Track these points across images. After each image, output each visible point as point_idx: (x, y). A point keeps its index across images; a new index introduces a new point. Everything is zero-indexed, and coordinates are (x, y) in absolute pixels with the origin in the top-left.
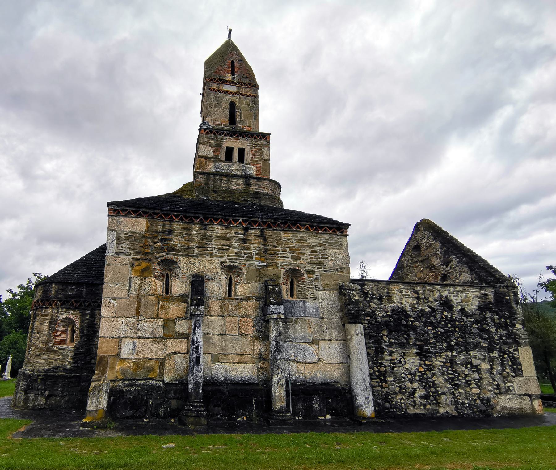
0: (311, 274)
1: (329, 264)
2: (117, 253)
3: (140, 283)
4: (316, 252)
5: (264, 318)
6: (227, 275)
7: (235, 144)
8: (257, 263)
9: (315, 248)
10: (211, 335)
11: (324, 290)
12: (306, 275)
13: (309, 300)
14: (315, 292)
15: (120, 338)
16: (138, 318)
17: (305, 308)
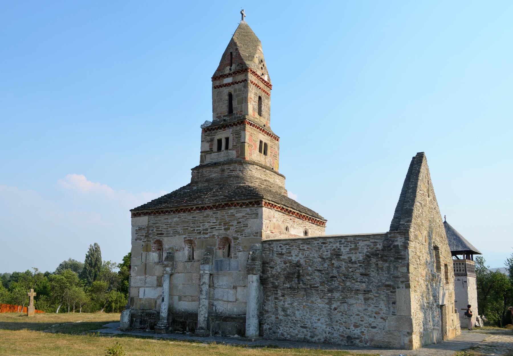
1: (247, 231)
4: (240, 223)
6: (191, 246)
7: (222, 135)
9: (240, 220)
12: (233, 241)
14: (238, 253)
15: (139, 287)
17: (229, 264)
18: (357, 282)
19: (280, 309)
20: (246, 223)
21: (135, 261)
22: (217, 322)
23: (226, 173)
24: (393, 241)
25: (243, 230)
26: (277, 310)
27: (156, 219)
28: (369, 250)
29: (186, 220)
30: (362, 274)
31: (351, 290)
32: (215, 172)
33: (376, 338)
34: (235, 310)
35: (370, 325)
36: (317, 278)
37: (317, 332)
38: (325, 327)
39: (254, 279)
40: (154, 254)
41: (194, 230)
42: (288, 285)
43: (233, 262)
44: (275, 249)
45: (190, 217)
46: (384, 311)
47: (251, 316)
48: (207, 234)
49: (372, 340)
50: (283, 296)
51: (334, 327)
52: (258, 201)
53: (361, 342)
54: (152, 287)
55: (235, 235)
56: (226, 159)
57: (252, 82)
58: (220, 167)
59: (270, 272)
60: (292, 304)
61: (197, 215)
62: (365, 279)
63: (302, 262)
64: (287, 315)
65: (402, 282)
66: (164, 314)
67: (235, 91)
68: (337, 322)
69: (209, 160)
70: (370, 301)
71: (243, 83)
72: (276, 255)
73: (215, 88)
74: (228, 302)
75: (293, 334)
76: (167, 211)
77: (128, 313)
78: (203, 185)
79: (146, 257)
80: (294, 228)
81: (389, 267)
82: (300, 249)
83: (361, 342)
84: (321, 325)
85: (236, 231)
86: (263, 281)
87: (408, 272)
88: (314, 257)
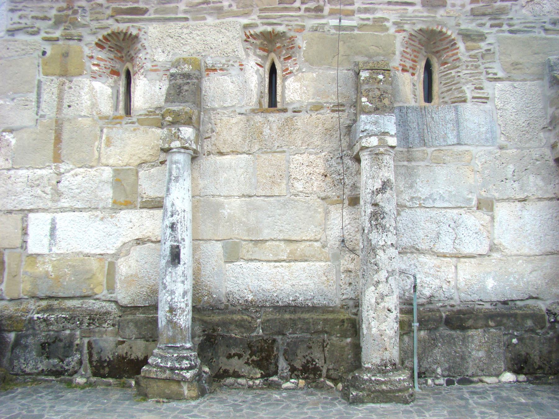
0: (473, 40)
2: (12, 32)
5: (350, 152)
6: (264, 58)
8: (334, 22)
10: (222, 199)
11: (509, 79)
12: (461, 45)
13: (468, 105)
14: (487, 85)
15: (25, 213)
16: (57, 167)
17: (457, 123)
25: (502, 11)
34: (490, 284)
40: (97, 85)
43: (473, 115)
54: (90, 209)
74: (459, 256)
79: (60, 98)
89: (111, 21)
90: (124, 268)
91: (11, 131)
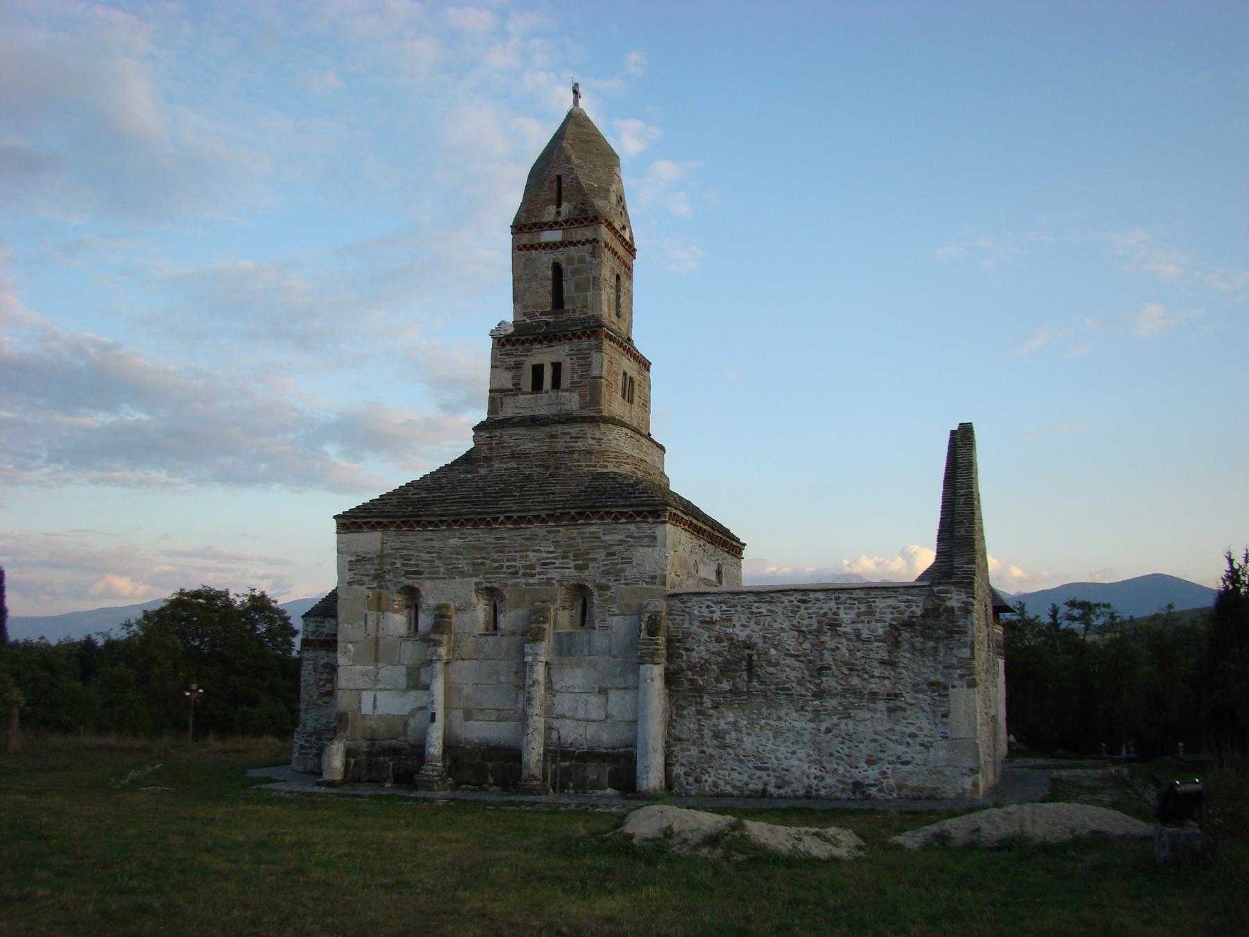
1: (630, 572)
3: (378, 618)
4: (613, 554)
7: (545, 356)
12: (596, 593)
14: (609, 619)
15: (360, 690)
17: (589, 643)
18: (873, 677)
19: (708, 733)
20: (627, 554)
21: (348, 631)
22: (563, 764)
23: (561, 445)
24: (943, 600)
25: (622, 570)
26: (702, 736)
27: (404, 539)
28: (896, 615)
29: (481, 544)
30: (882, 662)
31: (859, 694)
32: (534, 440)
33: (910, 783)
35: (899, 757)
36: (791, 672)
37: (789, 777)
38: (806, 765)
39: (655, 673)
41: (502, 567)
42: (726, 686)
44: (696, 612)
45: (490, 538)
46: (927, 732)
47: (650, 749)
48: (533, 575)
49: (900, 787)
50: (715, 707)
51: (825, 764)
52: (657, 511)
53: (881, 791)
54: (395, 690)
55: (603, 581)
56: (554, 410)
57: (607, 245)
58: (547, 429)
59: (685, 658)
60: (735, 724)
61: (508, 535)
62: (888, 672)
63: (756, 638)
64: (725, 746)
65: (961, 676)
66: (435, 748)
67: (570, 260)
68: (831, 755)
69: (509, 411)
70: (900, 713)
71: (588, 247)
72: (696, 623)
73: (520, 249)
74: (588, 721)
75: (738, 784)
76: (430, 523)
77: (342, 747)
78: (504, 466)
79: (378, 623)
80: (705, 564)
81: (935, 649)
82: (752, 613)
83: (881, 791)
84: (796, 763)
85: (605, 573)
86: (670, 679)
87: (973, 658)
88: (783, 630)
89: (403, 579)
90: (412, 723)
91: (351, 643)
